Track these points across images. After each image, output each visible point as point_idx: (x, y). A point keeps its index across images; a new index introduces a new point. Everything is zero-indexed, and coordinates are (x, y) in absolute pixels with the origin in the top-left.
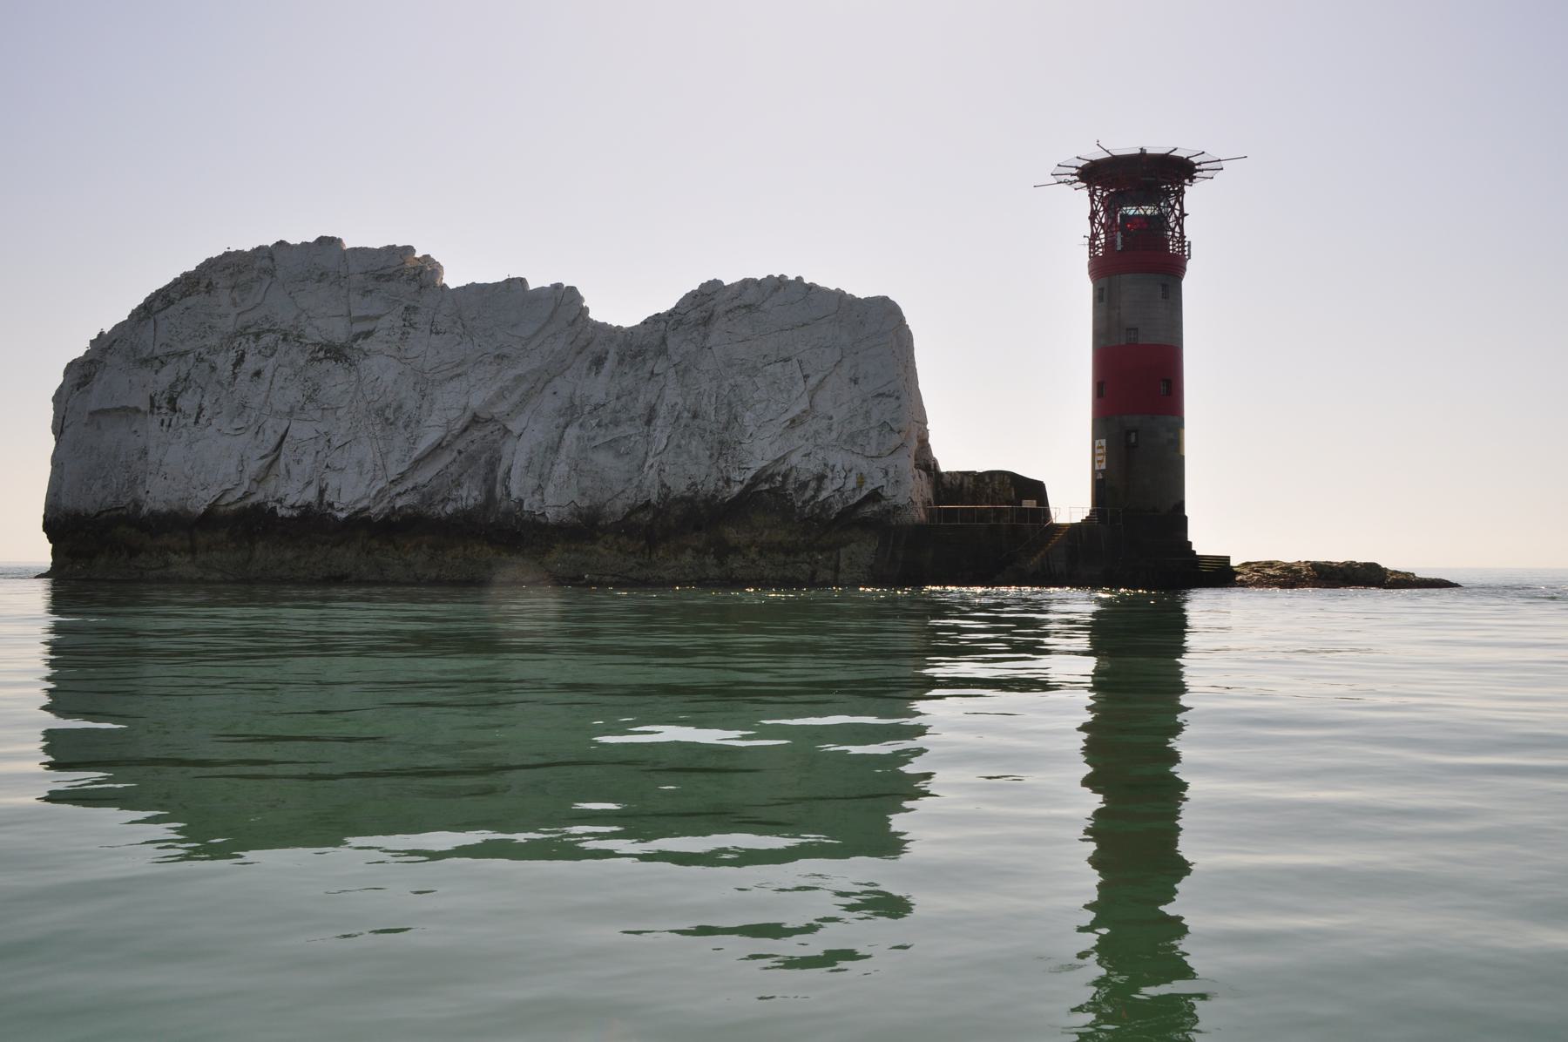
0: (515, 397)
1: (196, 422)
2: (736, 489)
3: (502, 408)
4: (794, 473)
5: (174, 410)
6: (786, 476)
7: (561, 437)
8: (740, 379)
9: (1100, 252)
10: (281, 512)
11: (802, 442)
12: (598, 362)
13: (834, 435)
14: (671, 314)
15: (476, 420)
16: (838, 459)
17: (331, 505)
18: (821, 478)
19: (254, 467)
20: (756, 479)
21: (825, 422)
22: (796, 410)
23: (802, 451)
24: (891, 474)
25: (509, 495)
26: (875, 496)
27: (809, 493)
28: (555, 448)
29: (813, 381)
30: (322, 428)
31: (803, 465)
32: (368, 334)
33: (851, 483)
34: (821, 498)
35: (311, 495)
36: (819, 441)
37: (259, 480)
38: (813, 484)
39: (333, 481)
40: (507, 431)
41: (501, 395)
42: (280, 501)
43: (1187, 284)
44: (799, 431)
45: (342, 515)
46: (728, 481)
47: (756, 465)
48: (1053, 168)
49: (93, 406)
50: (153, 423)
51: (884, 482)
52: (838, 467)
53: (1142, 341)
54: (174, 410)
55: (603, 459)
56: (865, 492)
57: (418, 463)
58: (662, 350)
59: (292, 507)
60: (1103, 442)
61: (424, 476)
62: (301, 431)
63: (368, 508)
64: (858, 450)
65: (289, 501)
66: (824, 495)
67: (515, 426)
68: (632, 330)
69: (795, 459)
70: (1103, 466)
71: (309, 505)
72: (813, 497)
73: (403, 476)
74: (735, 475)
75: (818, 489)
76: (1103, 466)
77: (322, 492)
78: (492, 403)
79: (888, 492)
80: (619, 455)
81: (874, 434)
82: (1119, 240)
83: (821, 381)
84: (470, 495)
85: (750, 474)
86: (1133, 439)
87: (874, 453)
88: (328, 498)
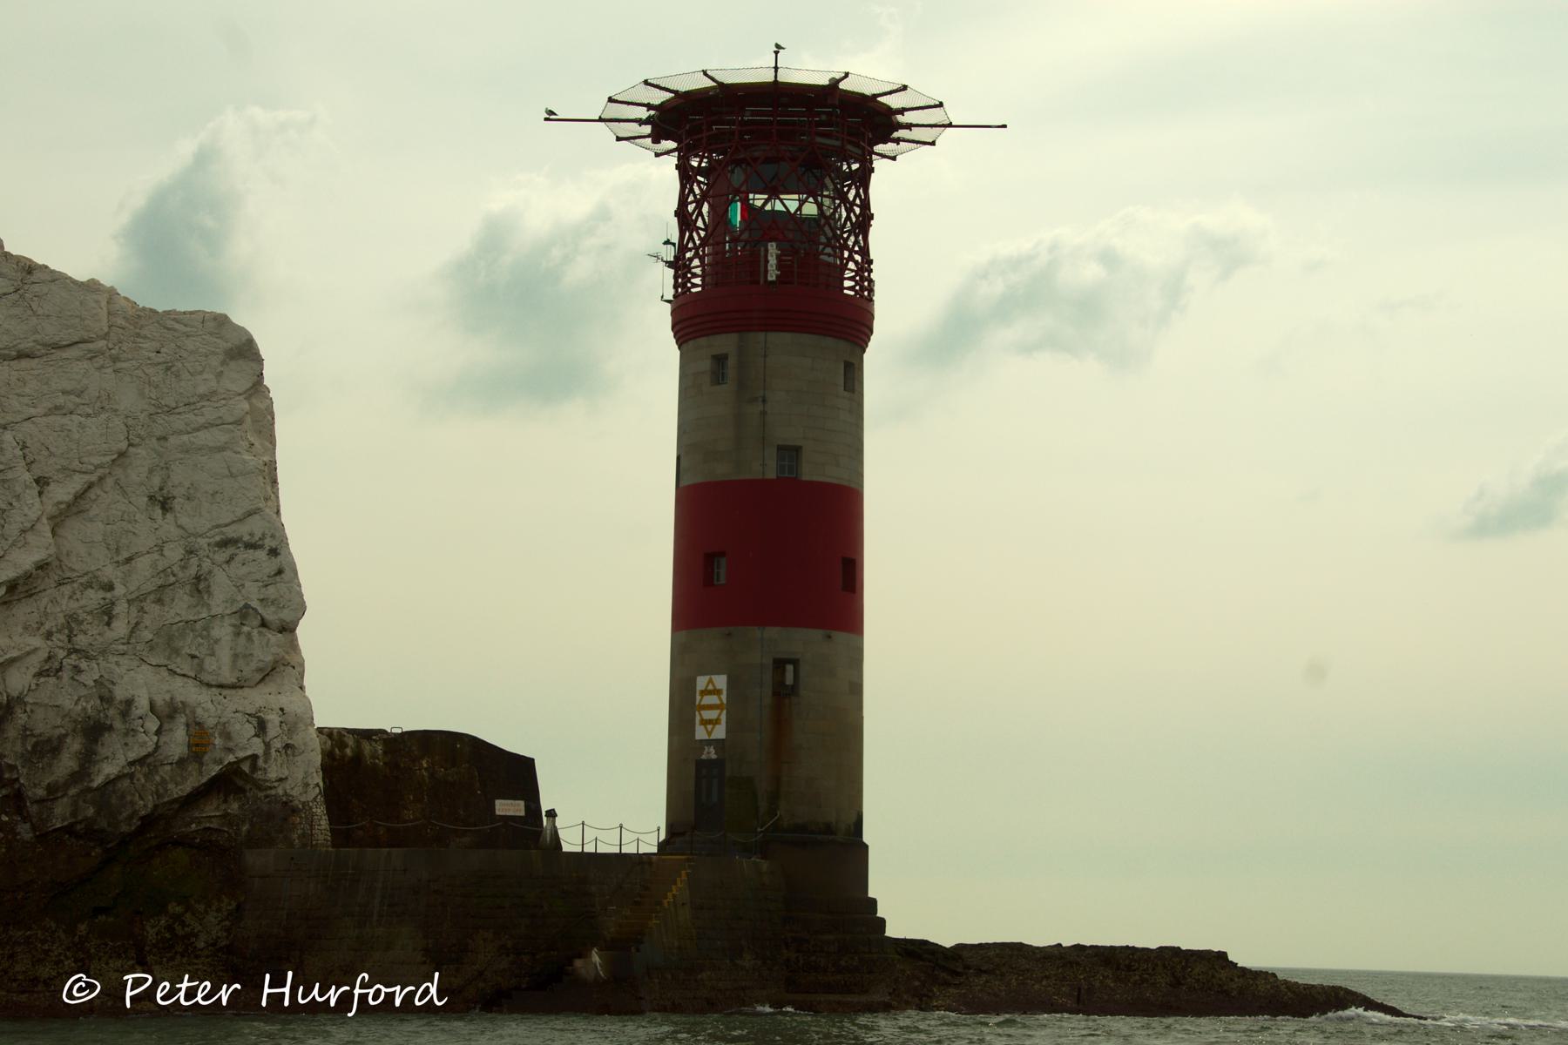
4: (21, 718)
11: (36, 641)
13: (120, 628)
16: (141, 684)
18: (94, 731)
21: (94, 597)
22: (24, 560)
23: (35, 662)
24: (273, 730)
26: (231, 781)
27: (66, 763)
29: (62, 492)
33: (177, 742)
34: (98, 781)
36: (81, 640)
38: (75, 745)
48: (626, 82)
51: (257, 747)
52: (142, 704)
53: (808, 473)
56: (215, 770)
60: (721, 681)
64: (185, 666)
66: (109, 770)
70: (720, 732)
72: (81, 774)
75: (88, 758)
76: (720, 732)
81: (223, 631)
82: (773, 261)
83: (80, 496)
86: (789, 680)
87: (228, 676)
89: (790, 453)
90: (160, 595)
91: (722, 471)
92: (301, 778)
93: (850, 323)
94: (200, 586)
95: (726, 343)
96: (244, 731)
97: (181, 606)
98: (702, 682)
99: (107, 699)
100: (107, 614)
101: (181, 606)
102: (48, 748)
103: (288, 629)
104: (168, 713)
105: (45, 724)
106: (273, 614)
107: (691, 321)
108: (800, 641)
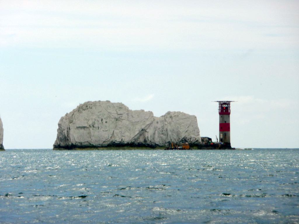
0: (147, 127)
1: (98, 129)
2: (180, 140)
3: (146, 128)
5: (94, 127)
6: (186, 138)
7: (155, 133)
8: (178, 126)
9: (220, 112)
10: (116, 142)
12: (158, 122)
14: (165, 116)
15: (142, 130)
16: (193, 136)
17: (124, 141)
18: (191, 138)
19: (110, 136)
20: (183, 138)
22: (187, 130)
25: (148, 140)
26: (197, 141)
27: (189, 140)
28: (154, 134)
29: (188, 126)
30: (120, 130)
31: (188, 137)
32: (121, 117)
33: (194, 139)
35: (120, 140)
37: (111, 138)
39: (123, 138)
40: (146, 131)
41: (146, 127)
42: (116, 141)
43: (231, 115)
44: (187, 132)
45: (126, 143)
46: (179, 139)
47: (183, 137)
49: (78, 126)
50: (91, 129)
53: (227, 122)
54: (94, 127)
55: (162, 136)
57: (135, 136)
58: (165, 121)
59: (118, 142)
61: (136, 138)
62: (116, 131)
63: (129, 142)
65: (118, 141)
67: (147, 131)
68: (159, 118)
69: (187, 136)
71: (120, 142)
72: (190, 141)
73: (133, 137)
74: (180, 138)
77: (122, 140)
78: (145, 128)
79: (199, 140)
80: (164, 135)
84: (141, 140)
85: (182, 138)
88: (123, 140)
89: (225, 122)
90: (193, 131)
91: (222, 123)
92: (200, 141)
93: (229, 114)
94: (195, 131)
95: (222, 115)
96: (197, 138)
97: (194, 132)
98: (221, 134)
99: (191, 137)
100: (190, 132)
101: (194, 132)
102: (188, 139)
103: (199, 133)
104: (194, 137)
105: (188, 138)
106: (198, 132)
107: (220, 114)
108: (226, 132)
